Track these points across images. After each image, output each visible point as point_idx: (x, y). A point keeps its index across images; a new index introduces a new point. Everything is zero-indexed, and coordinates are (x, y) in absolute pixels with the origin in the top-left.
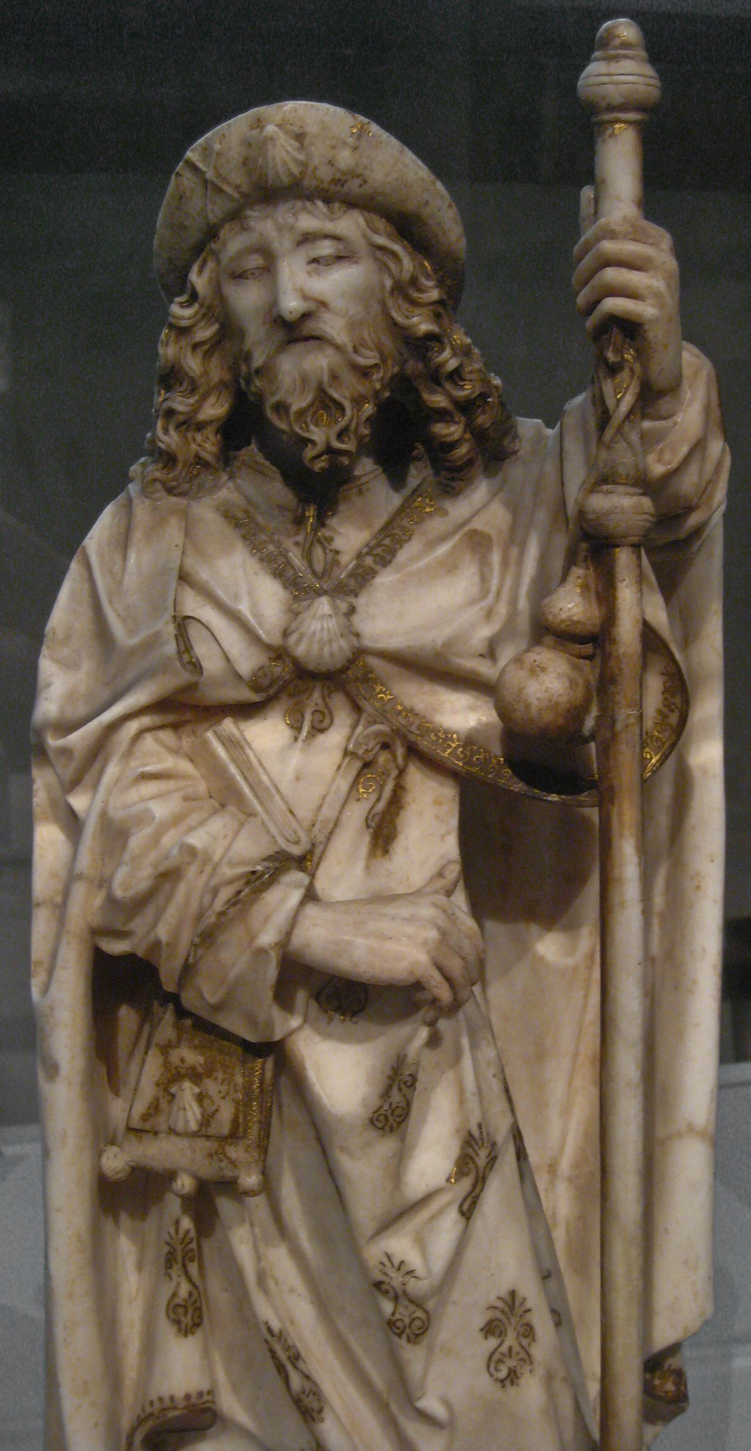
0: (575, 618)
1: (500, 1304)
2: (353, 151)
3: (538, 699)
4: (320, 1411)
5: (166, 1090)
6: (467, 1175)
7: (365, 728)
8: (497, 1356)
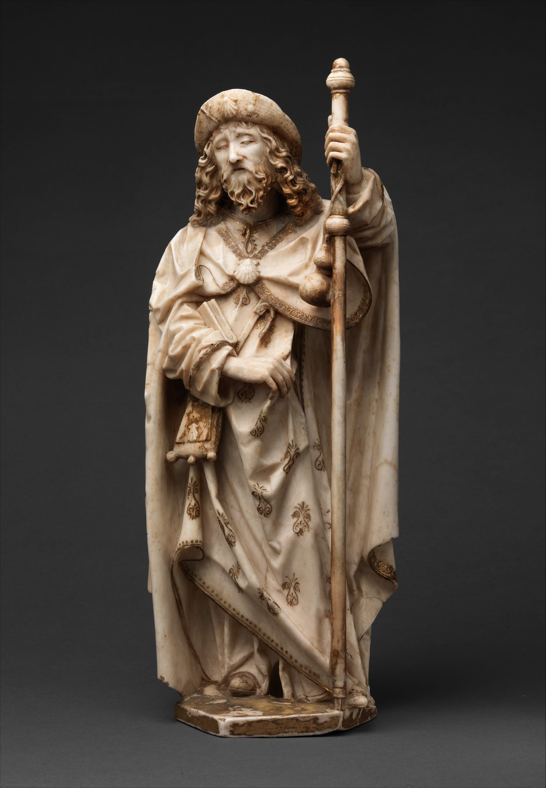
0: (322, 261)
1: (299, 506)
3: (310, 288)
4: (234, 542)
5: (188, 427)
7: (260, 303)
8: (296, 524)
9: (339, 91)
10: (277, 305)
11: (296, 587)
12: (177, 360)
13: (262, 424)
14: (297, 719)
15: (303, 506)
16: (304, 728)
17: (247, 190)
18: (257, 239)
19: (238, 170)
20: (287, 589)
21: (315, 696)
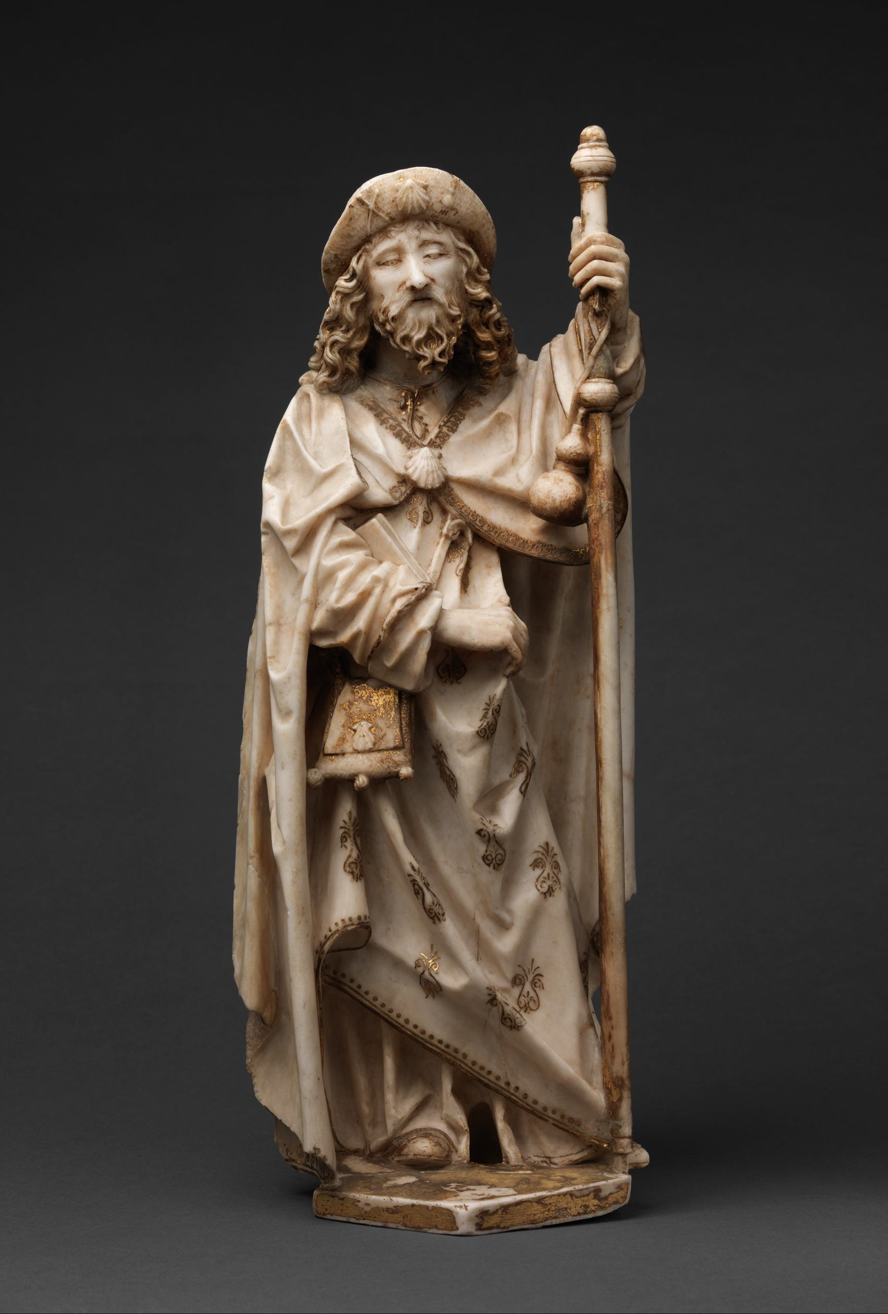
0: (578, 452)
1: (541, 850)
3: (560, 496)
4: (443, 914)
6: (522, 772)
8: (541, 879)
9: (599, 179)
10: (477, 522)
11: (536, 981)
12: (343, 616)
13: (495, 718)
14: (571, 1194)
15: (548, 849)
16: (581, 1207)
17: (434, 335)
18: (425, 415)
20: (518, 985)
21: (567, 1155)
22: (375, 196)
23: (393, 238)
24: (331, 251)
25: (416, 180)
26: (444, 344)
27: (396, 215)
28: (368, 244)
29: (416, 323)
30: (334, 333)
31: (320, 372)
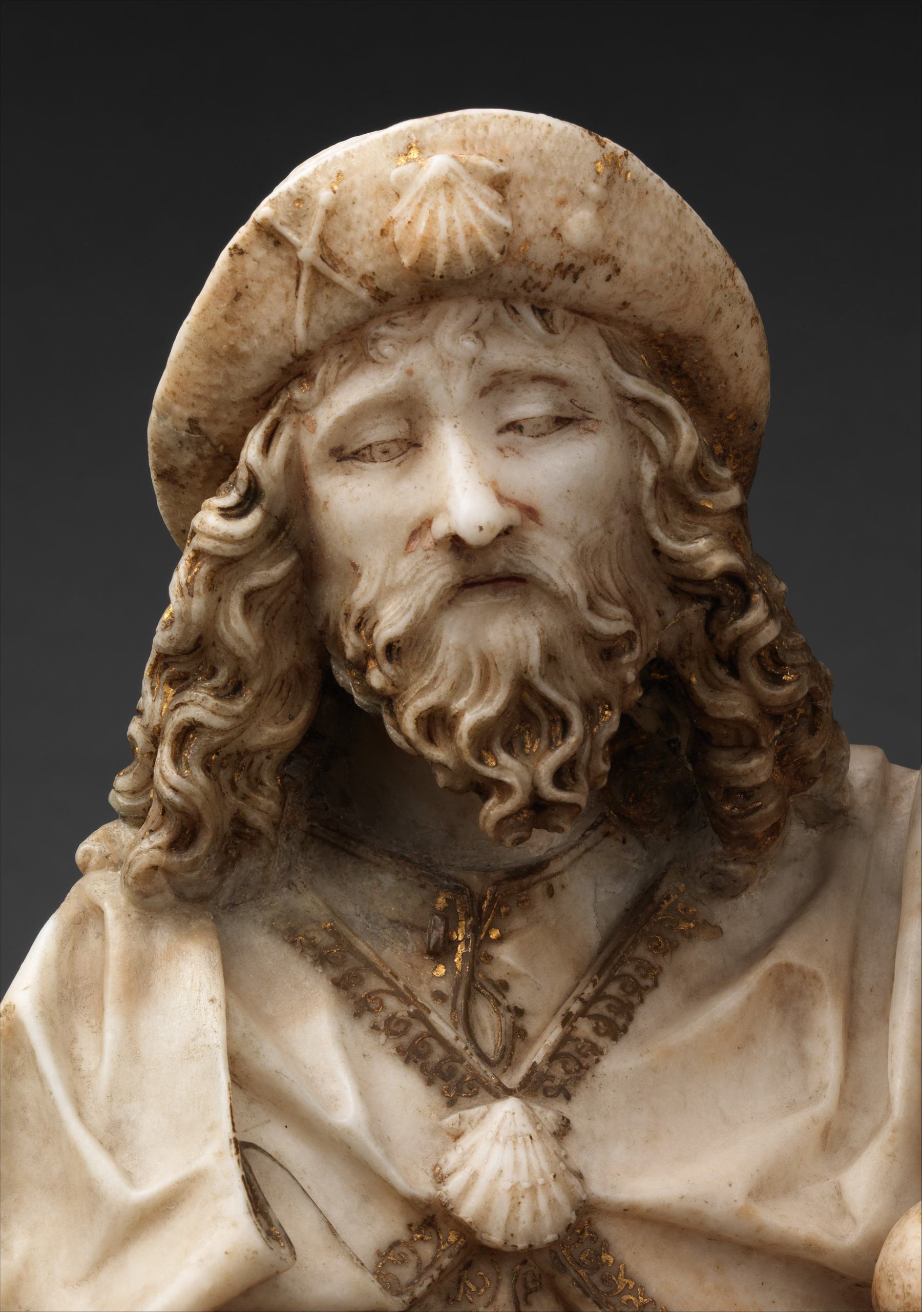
2: (598, 210)
17: (535, 707)
18: (517, 975)
19: (489, 587)
22: (320, 214)
23: (389, 363)
24: (177, 408)
25: (464, 157)
26: (572, 740)
27: (396, 283)
28: (301, 385)
29: (470, 664)
30: (188, 695)
31: (145, 827)
